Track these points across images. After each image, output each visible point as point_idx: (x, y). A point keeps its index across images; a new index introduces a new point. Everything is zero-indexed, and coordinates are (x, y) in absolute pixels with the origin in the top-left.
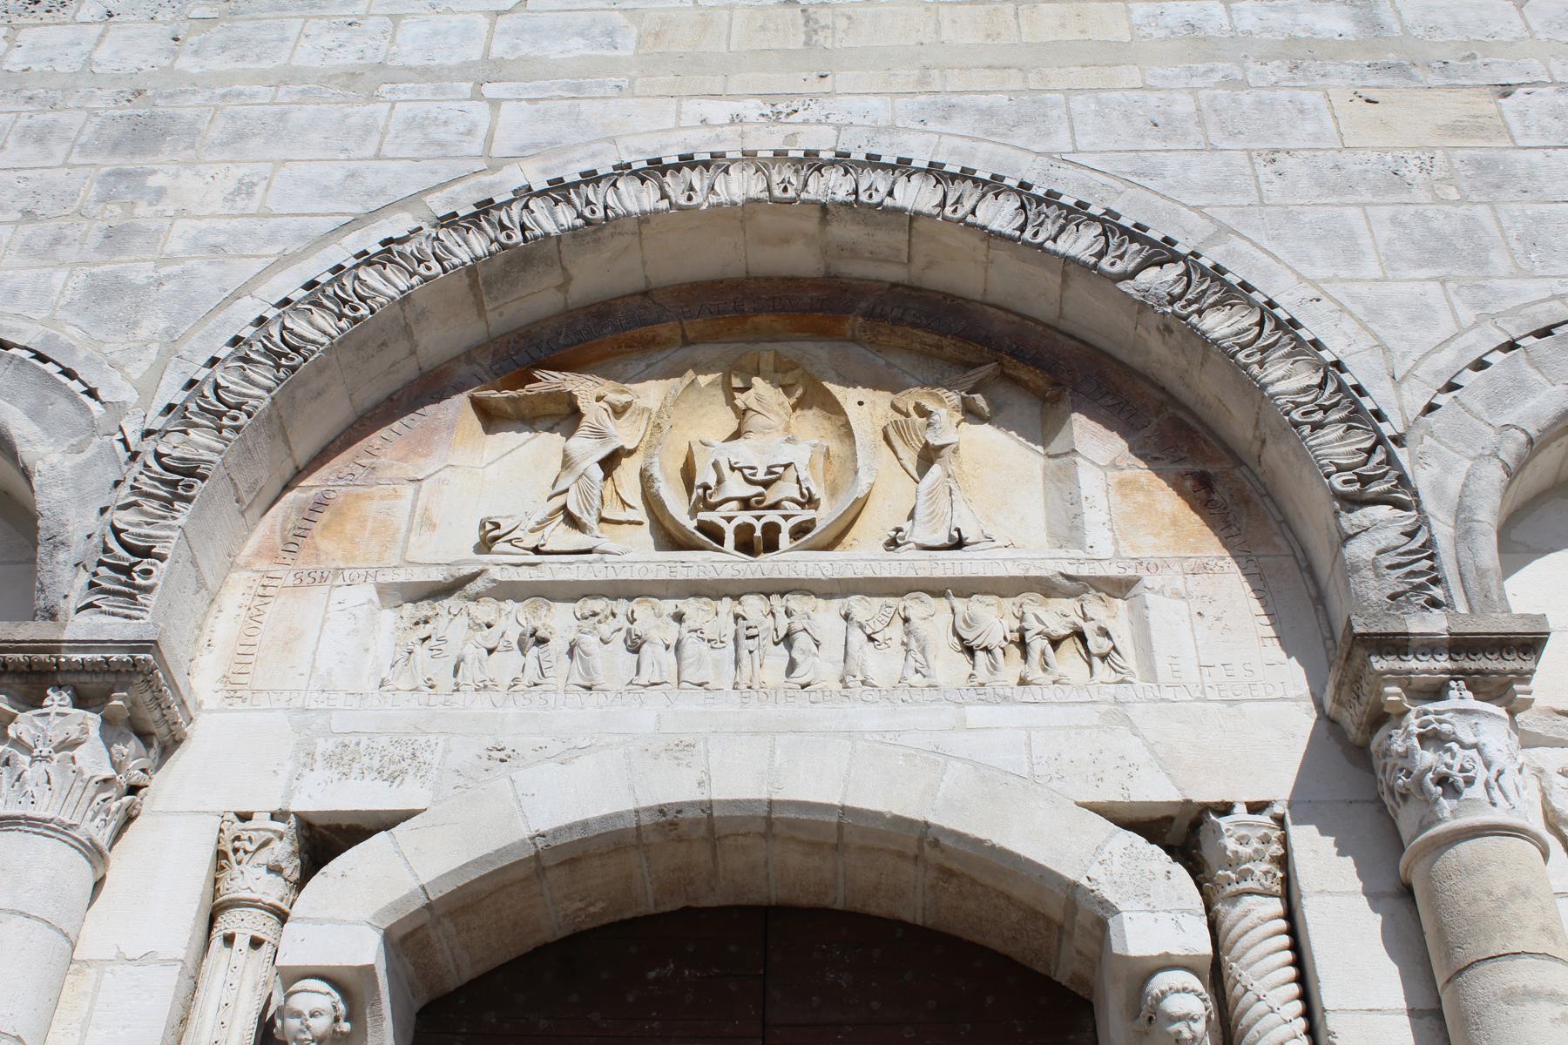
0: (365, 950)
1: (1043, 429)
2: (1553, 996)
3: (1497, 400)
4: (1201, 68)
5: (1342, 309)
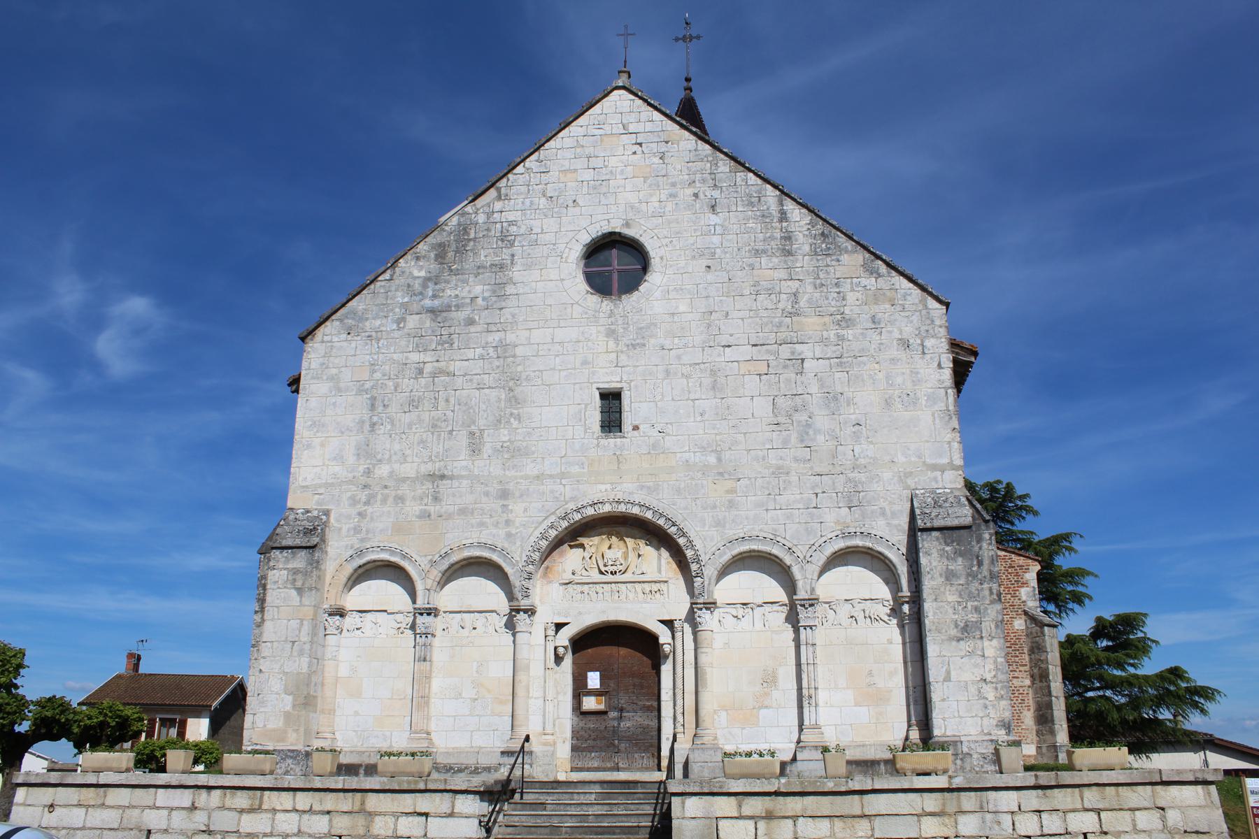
0: (567, 643)
1: (658, 549)
2: (706, 653)
3: (721, 556)
4: (687, 474)
5: (701, 538)
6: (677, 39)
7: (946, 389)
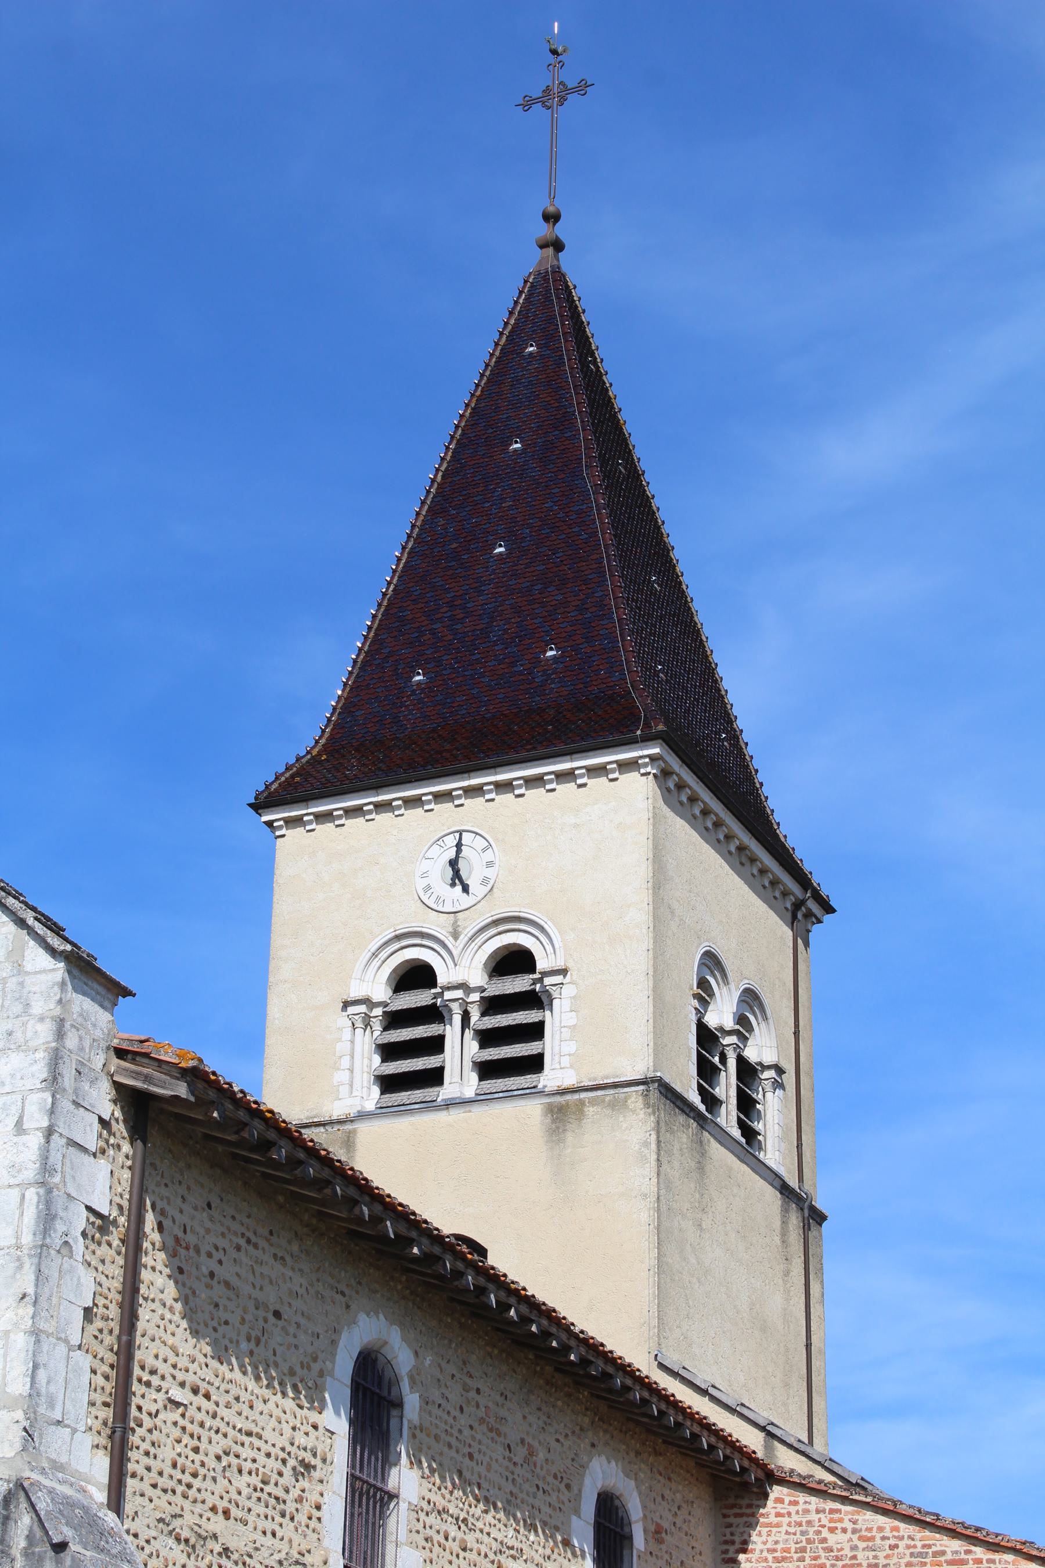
6: (527, 104)
7: (23, 1186)
